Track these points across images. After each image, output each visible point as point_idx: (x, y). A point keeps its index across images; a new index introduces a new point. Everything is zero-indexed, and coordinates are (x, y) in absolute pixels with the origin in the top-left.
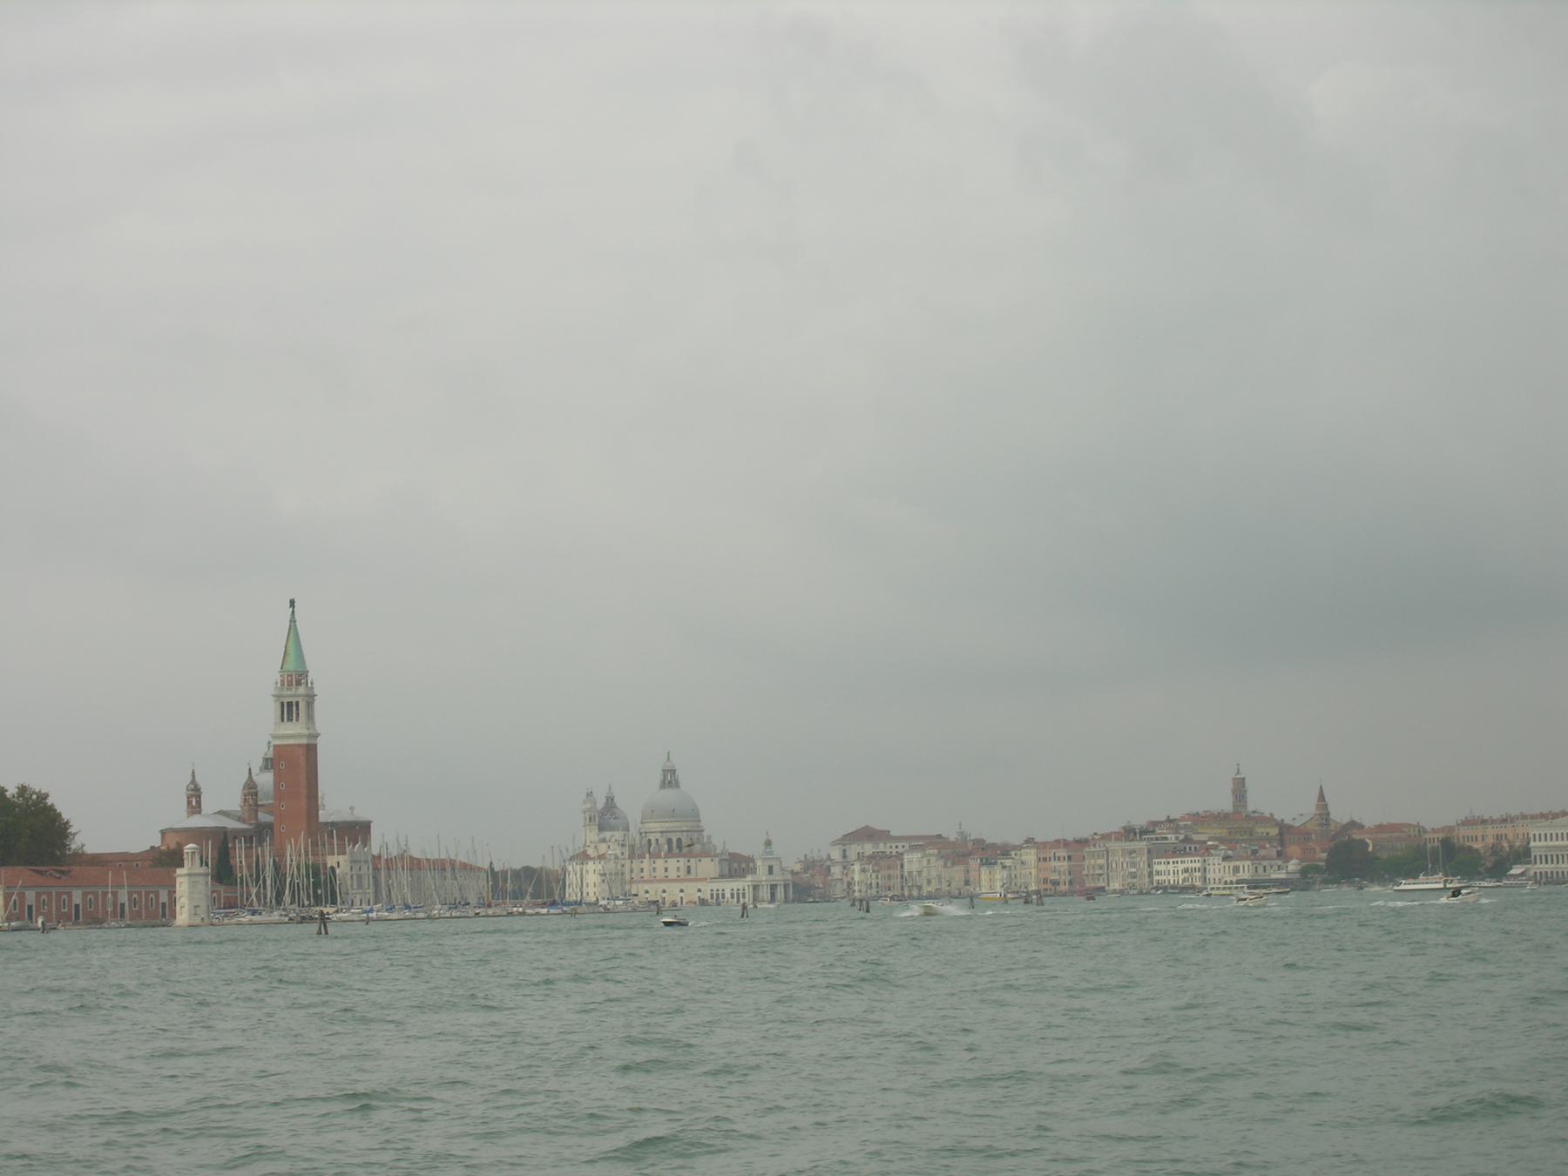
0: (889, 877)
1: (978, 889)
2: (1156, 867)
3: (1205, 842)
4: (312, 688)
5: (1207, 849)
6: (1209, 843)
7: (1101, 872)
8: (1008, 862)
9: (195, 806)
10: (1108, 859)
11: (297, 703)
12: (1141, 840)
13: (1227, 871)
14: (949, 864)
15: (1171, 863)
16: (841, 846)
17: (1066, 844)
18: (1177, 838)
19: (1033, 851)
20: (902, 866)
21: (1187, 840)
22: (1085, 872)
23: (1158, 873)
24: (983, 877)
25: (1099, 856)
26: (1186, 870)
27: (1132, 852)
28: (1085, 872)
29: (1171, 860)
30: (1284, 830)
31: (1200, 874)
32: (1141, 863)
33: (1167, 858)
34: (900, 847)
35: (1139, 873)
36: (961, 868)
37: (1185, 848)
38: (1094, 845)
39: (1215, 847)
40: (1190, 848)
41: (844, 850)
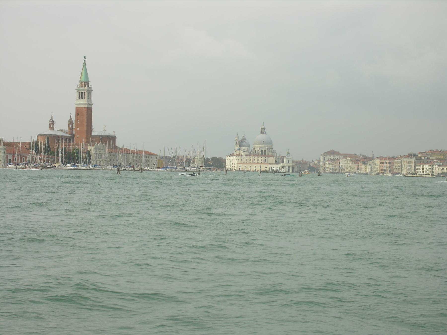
0: (336, 166)
1: (361, 171)
2: (417, 167)
3: (434, 159)
5: (434, 162)
6: (435, 160)
7: (399, 168)
8: (371, 163)
10: (401, 164)
12: (413, 158)
13: (439, 170)
14: (353, 163)
15: (422, 166)
16: (323, 156)
17: (389, 158)
18: (425, 158)
19: (379, 160)
20: (340, 163)
21: (428, 159)
22: (394, 168)
23: (417, 169)
24: (363, 168)
25: (399, 163)
26: (426, 169)
27: (409, 162)
28: (394, 168)
29: (422, 165)
31: (431, 170)
32: (412, 166)
33: (420, 164)
34: (340, 157)
35: (411, 169)
36: (356, 164)
37: (427, 161)
38: (398, 159)
39: (436, 162)
40: (429, 162)
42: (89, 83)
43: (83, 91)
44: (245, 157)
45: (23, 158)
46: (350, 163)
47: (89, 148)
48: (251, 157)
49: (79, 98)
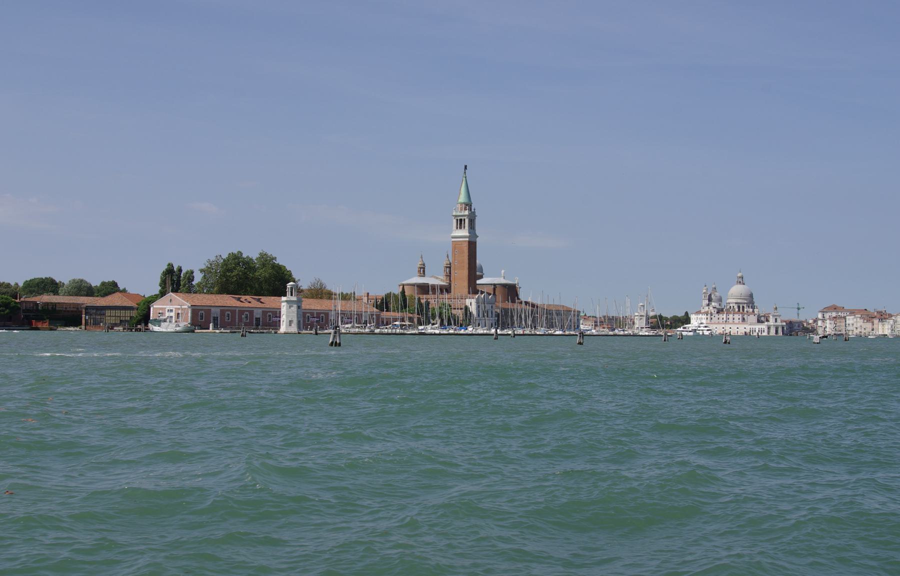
14: (865, 321)
20: (846, 321)
24: (880, 327)
41: (823, 315)
42: (471, 205)
43: (463, 218)
44: (717, 315)
46: (860, 322)
47: (468, 302)
48: (725, 315)
49: (457, 228)
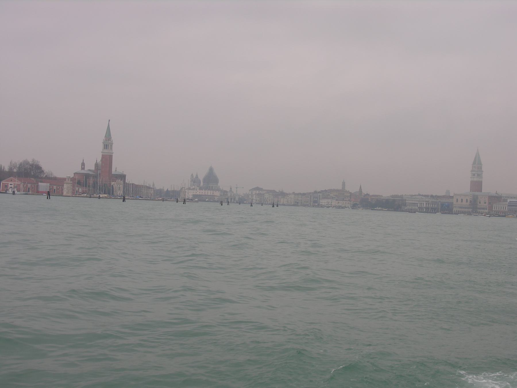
4: (112, 141)
9: (83, 168)
11: (108, 145)
30: (351, 193)
39: (335, 197)
41: (252, 192)
45: (33, 187)
